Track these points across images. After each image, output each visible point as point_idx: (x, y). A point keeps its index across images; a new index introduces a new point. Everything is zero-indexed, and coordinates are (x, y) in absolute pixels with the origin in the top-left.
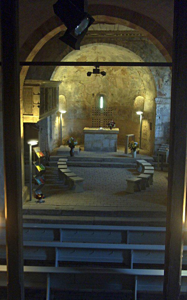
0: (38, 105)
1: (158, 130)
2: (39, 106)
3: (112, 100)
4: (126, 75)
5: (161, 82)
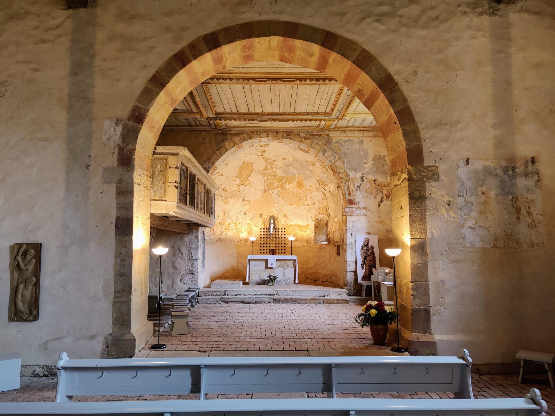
0: (176, 184)
1: (351, 250)
2: (176, 187)
3: (286, 222)
4: (302, 188)
5: (351, 188)
